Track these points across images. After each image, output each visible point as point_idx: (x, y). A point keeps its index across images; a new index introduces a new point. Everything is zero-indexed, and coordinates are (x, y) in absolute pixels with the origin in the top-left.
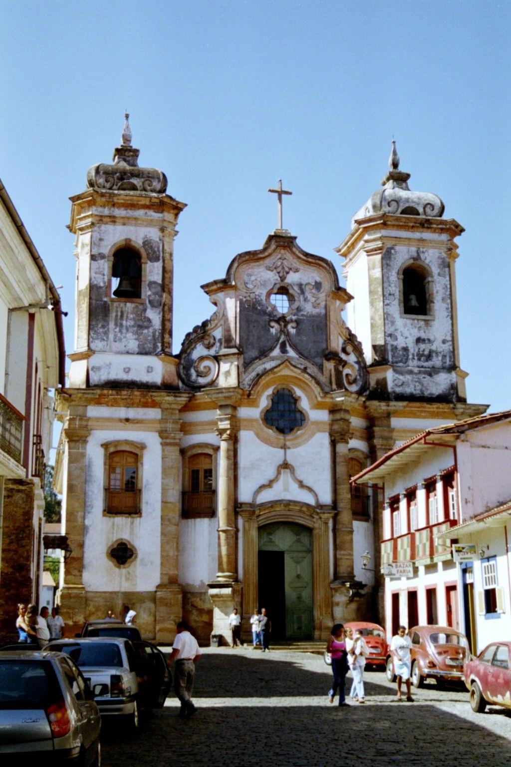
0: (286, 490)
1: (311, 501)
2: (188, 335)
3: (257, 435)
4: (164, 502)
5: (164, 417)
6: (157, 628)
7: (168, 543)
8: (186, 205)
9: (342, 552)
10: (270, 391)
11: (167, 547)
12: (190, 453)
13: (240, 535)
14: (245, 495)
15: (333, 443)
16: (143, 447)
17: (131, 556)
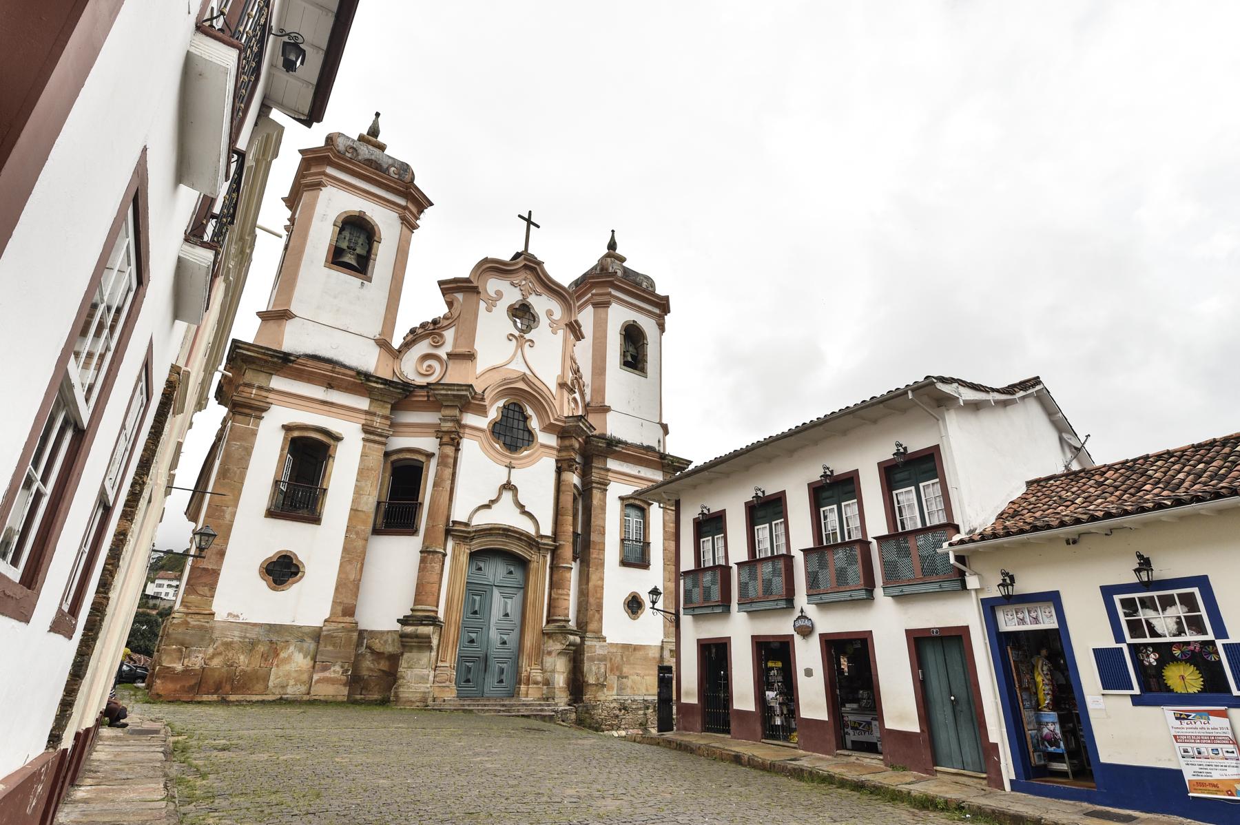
0: (505, 515)
1: (532, 532)
2: (413, 331)
3: (483, 449)
4: (354, 511)
5: (372, 410)
6: (316, 677)
7: (350, 561)
8: (431, 204)
9: (560, 591)
10: (501, 403)
11: (348, 568)
12: (394, 457)
13: (448, 560)
14: (460, 513)
15: (559, 471)
16: (338, 439)
17: (296, 574)
